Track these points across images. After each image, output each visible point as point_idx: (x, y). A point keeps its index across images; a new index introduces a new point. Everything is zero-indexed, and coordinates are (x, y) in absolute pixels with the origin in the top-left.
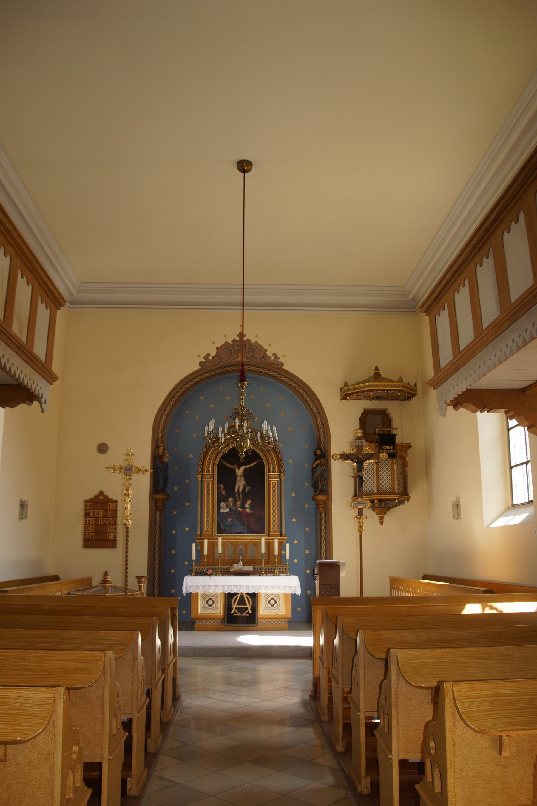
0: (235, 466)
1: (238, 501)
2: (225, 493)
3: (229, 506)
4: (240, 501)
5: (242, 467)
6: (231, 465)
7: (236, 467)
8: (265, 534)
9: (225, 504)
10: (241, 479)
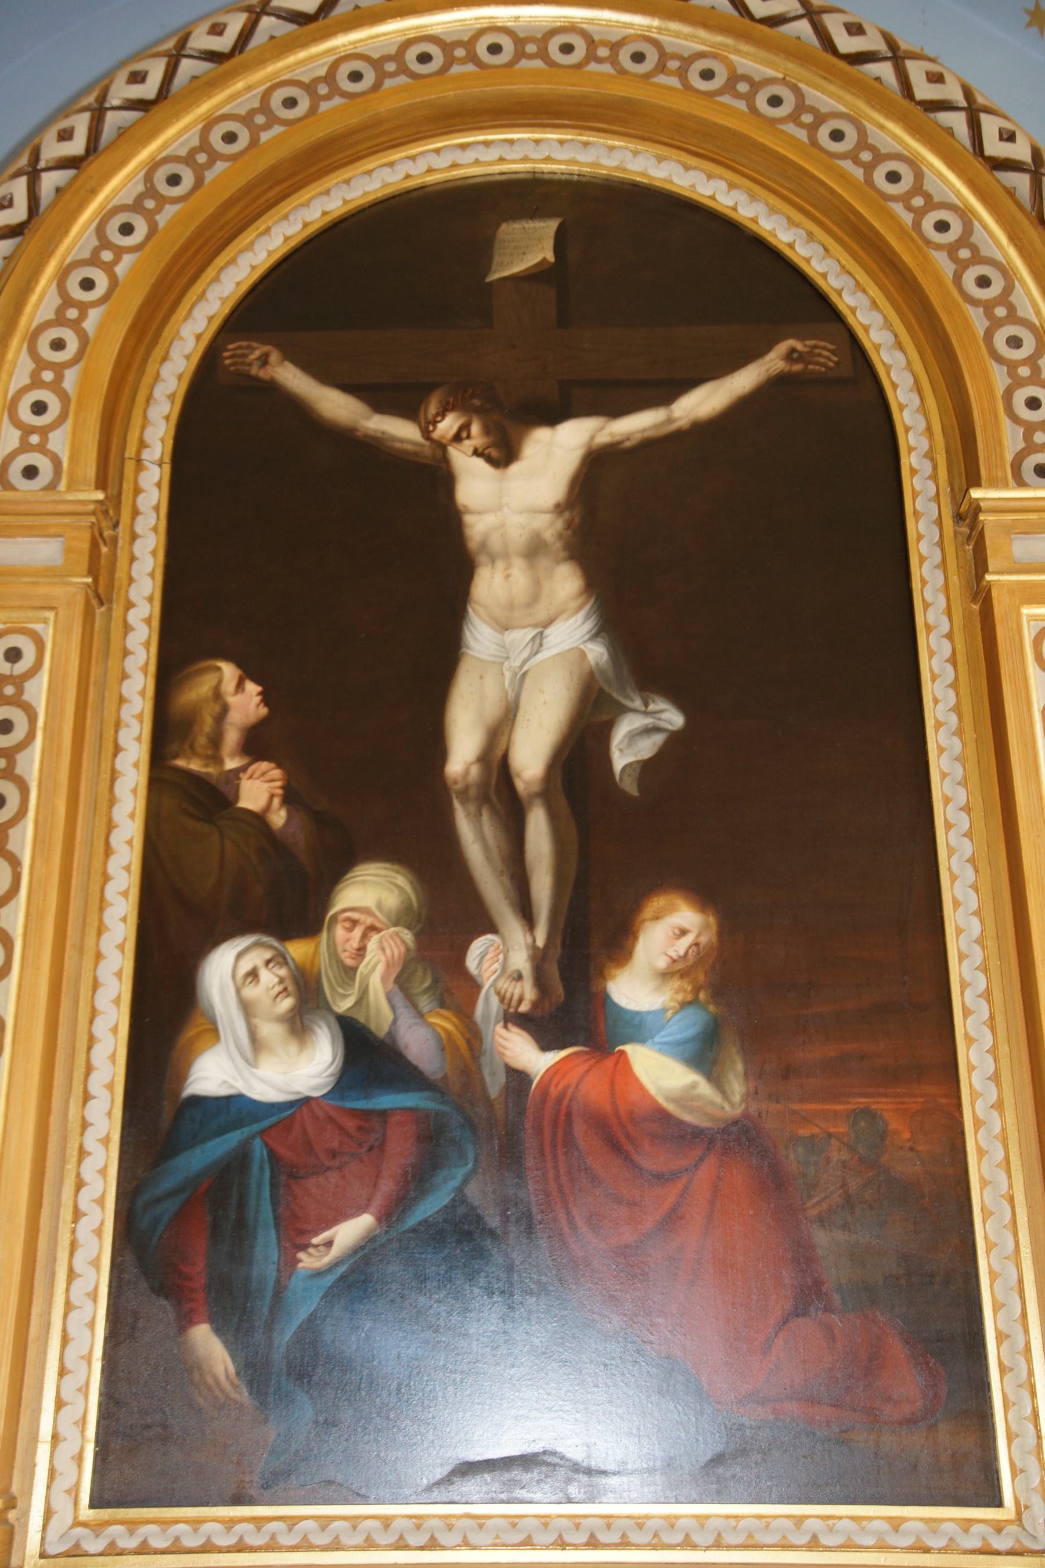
0: (448, 425)
1: (493, 929)
2: (290, 797)
3: (343, 1006)
4: (527, 914)
5: (541, 435)
6: (380, 406)
7: (457, 438)
8: (1000, 1504)
9: (280, 959)
10: (534, 599)
